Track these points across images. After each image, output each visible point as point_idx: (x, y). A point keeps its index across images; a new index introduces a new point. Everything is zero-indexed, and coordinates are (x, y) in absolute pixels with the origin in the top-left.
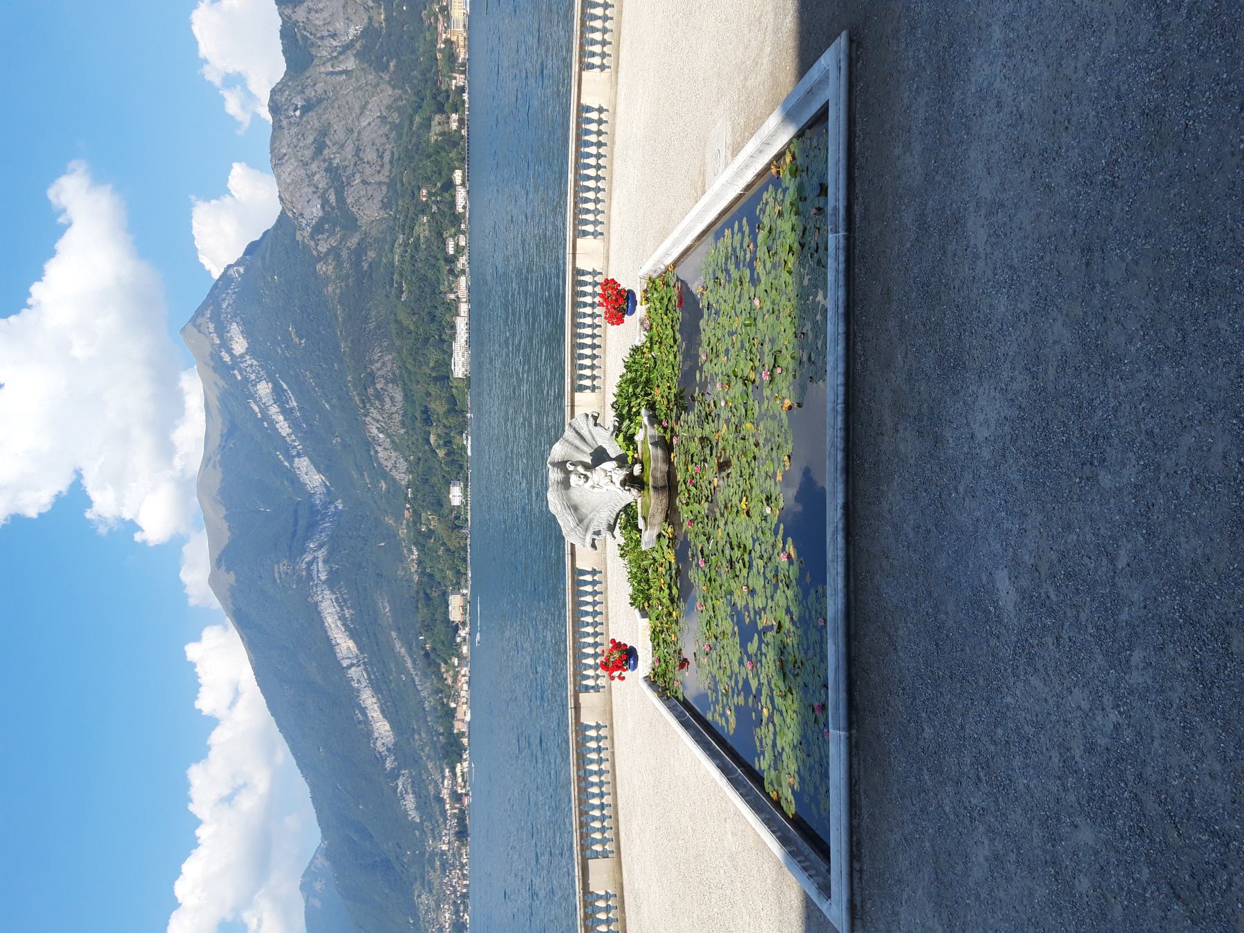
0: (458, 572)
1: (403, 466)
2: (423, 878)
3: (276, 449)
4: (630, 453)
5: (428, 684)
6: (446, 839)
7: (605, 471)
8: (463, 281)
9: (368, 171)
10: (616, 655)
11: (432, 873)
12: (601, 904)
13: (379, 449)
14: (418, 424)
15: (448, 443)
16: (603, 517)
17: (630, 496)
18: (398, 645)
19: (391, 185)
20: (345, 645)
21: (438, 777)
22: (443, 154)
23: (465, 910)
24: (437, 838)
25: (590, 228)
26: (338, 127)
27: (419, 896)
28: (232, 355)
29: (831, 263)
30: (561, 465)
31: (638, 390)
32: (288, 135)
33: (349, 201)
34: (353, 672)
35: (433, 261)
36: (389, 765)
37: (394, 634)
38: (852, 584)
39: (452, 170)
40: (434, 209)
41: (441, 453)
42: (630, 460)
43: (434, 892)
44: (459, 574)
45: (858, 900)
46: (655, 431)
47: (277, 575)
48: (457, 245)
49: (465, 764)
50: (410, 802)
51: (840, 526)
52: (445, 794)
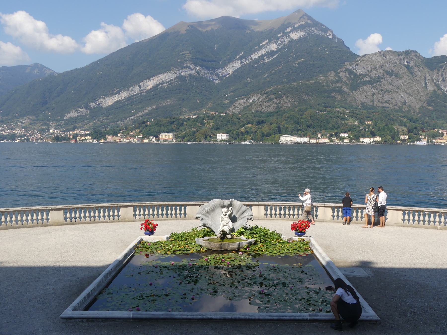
0: (184, 138)
1: (236, 111)
2: (38, 120)
3: (245, 52)
4: (236, 233)
5: (130, 123)
6: (55, 132)
7: (228, 223)
8: (327, 141)
9: (380, 96)
10: (151, 227)
11: (39, 124)
12: (45, 217)
13: (244, 100)
14: (257, 119)
15: (247, 133)
16: (210, 223)
17: (218, 233)
18: (149, 109)
19: (373, 107)
20: (150, 84)
21: (85, 128)
22: (388, 132)
23: (21, 140)
24: (56, 127)
25: (336, 214)
26: (400, 82)
27: (29, 119)
28: (289, 32)
29: (299, 314)
30: (231, 205)
31: (262, 237)
32: (394, 58)
33: (365, 87)
34: (137, 88)
35: (337, 126)
36: (92, 105)
37: (154, 107)
38: (184, 321)
39: (380, 136)
40: (362, 127)
41: (242, 129)
42: (233, 234)
43: (31, 126)
44: (183, 138)
45: (73, 321)
46: (245, 244)
47: (184, 52)
48: (344, 138)
49: (91, 141)
50: (74, 114)
51: (205, 317)
52: (77, 131)
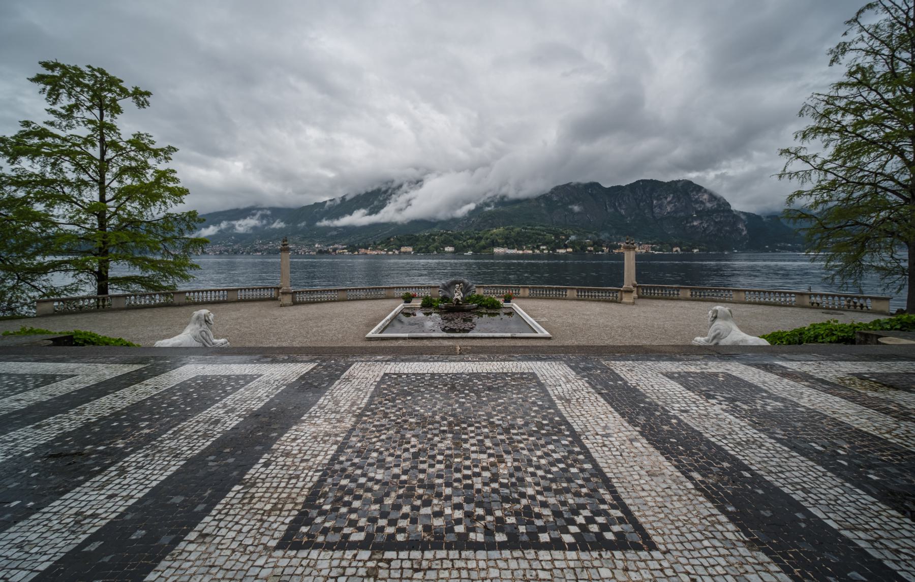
8: (530, 252)
15: (469, 246)
52: (336, 246)
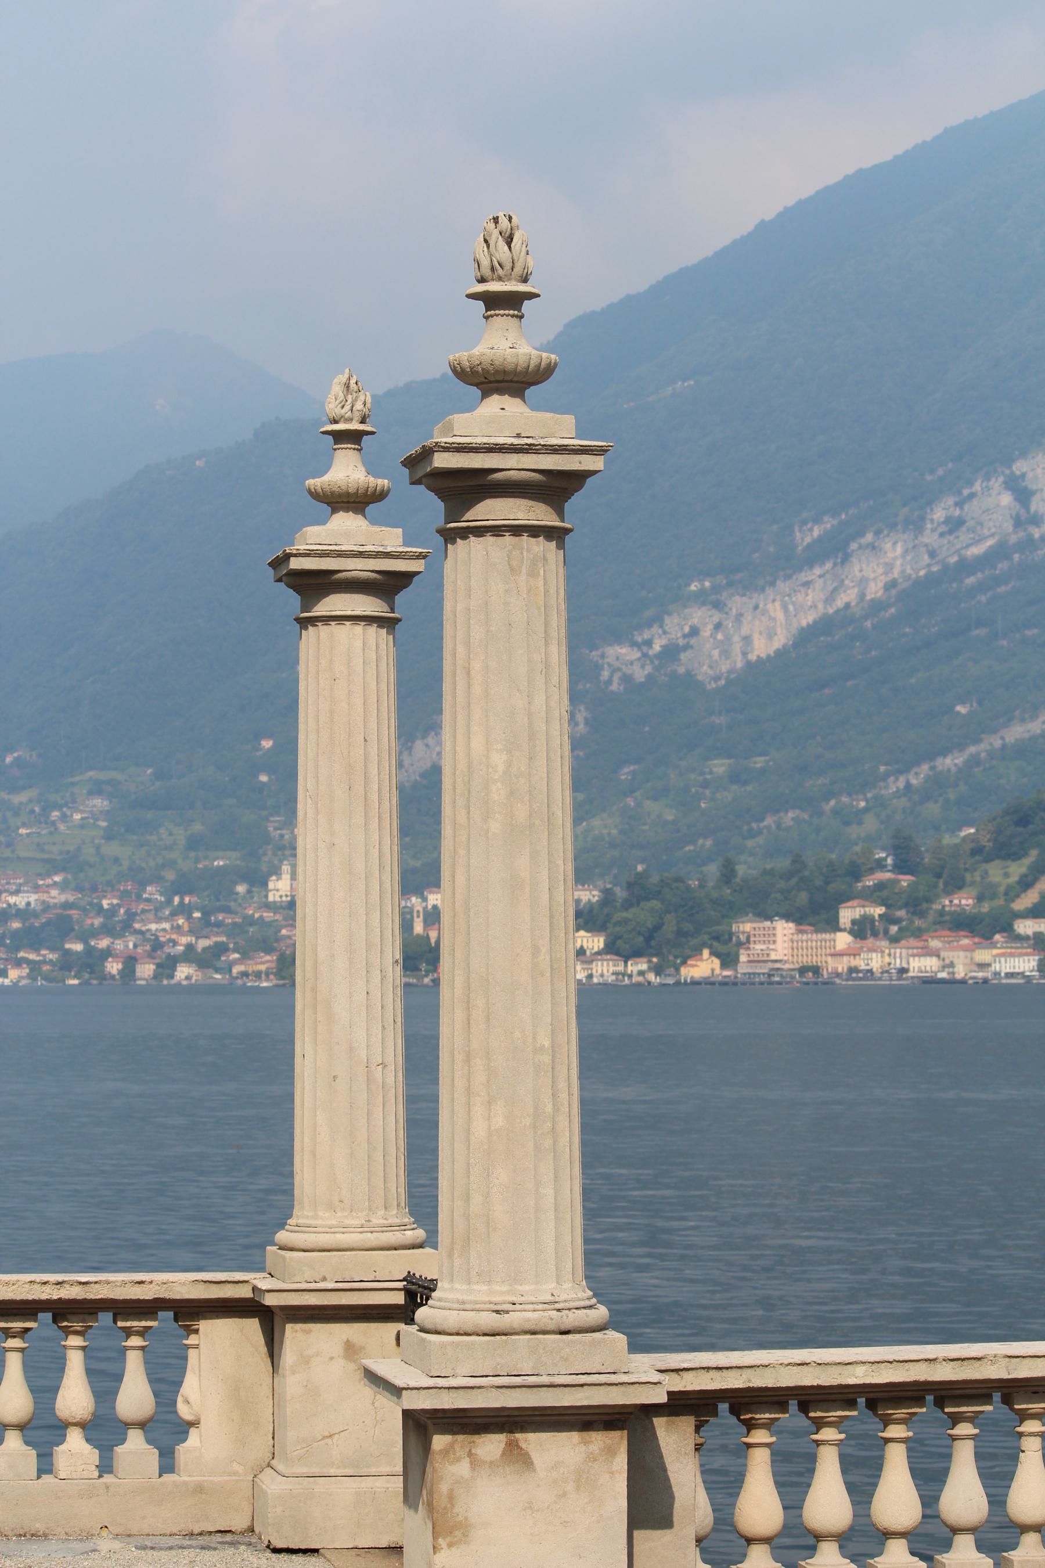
34: (994, 505)
